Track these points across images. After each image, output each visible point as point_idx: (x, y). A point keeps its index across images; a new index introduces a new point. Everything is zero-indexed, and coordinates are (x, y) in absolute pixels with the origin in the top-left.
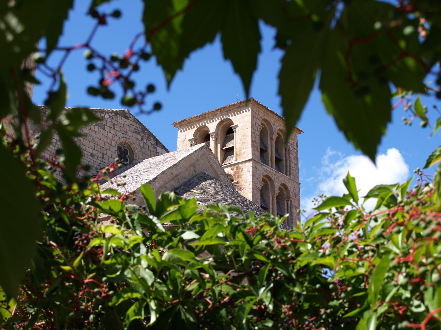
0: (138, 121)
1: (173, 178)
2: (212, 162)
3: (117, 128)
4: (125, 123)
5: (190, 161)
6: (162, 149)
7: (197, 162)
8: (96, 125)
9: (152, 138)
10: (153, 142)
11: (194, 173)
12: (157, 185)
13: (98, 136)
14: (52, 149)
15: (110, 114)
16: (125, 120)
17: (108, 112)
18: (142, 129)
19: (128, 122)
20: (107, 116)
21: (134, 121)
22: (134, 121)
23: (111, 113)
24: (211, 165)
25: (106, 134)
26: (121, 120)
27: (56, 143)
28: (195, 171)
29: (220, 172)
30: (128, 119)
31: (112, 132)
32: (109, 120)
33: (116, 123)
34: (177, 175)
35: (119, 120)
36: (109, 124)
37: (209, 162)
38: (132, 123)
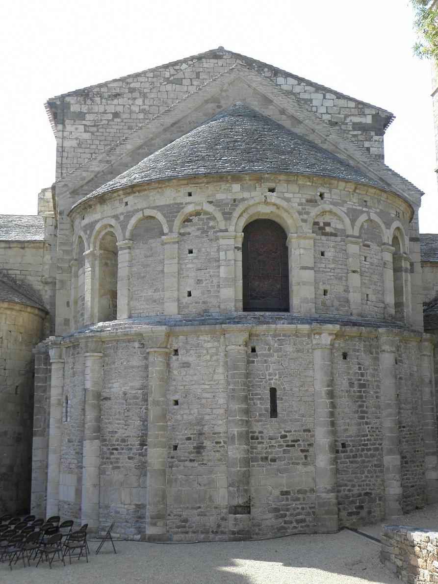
0: (239, 55)
1: (165, 130)
2: (254, 85)
3: (202, 76)
4: (216, 65)
5: (204, 96)
6: (286, 78)
7: (224, 94)
8: (168, 83)
9: (266, 70)
10: (268, 74)
11: (218, 110)
12: (129, 147)
13: (172, 96)
14: (103, 133)
15: (190, 62)
16: (215, 61)
17: (185, 61)
18: (246, 63)
19: (220, 62)
20: (184, 66)
21: (231, 58)
22: (231, 58)
23: (192, 60)
24: (255, 89)
25: (185, 89)
26: (208, 64)
27: (108, 124)
28: (219, 107)
29: (272, 93)
30: (222, 58)
31: (195, 83)
32: (189, 70)
33: (201, 70)
34: (174, 124)
35: (205, 65)
36: (187, 75)
37: (249, 86)
38: (228, 61)
